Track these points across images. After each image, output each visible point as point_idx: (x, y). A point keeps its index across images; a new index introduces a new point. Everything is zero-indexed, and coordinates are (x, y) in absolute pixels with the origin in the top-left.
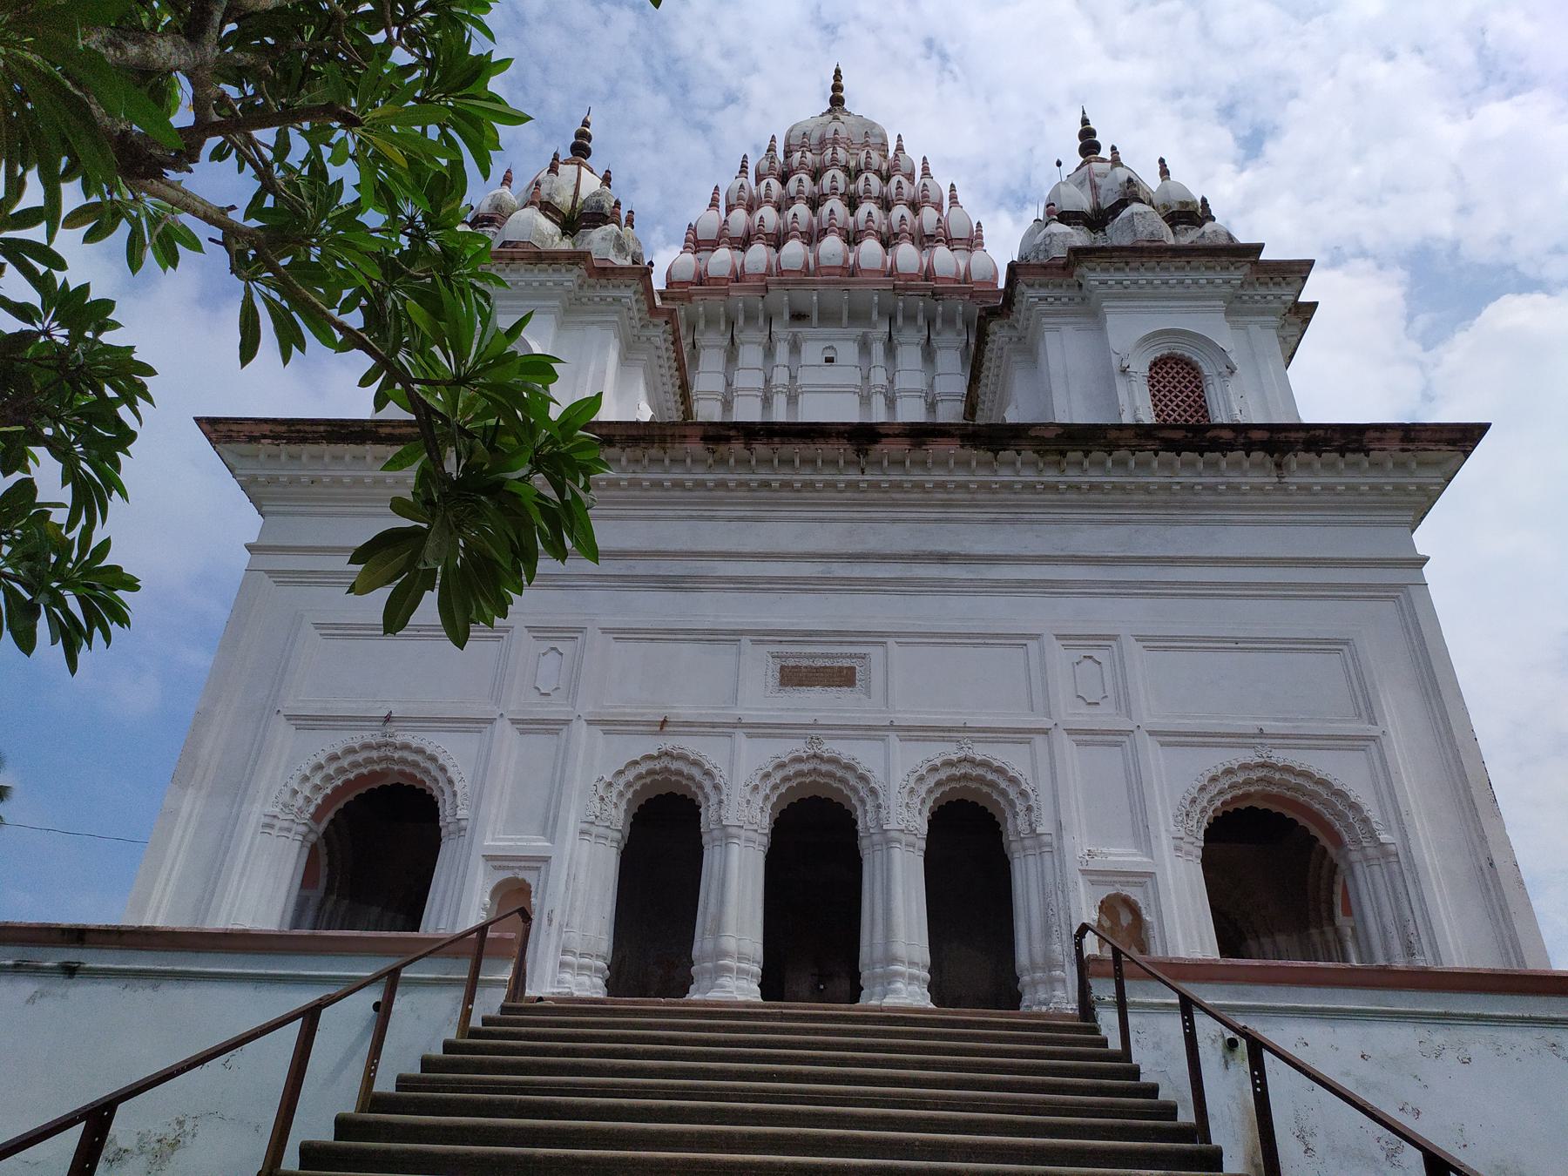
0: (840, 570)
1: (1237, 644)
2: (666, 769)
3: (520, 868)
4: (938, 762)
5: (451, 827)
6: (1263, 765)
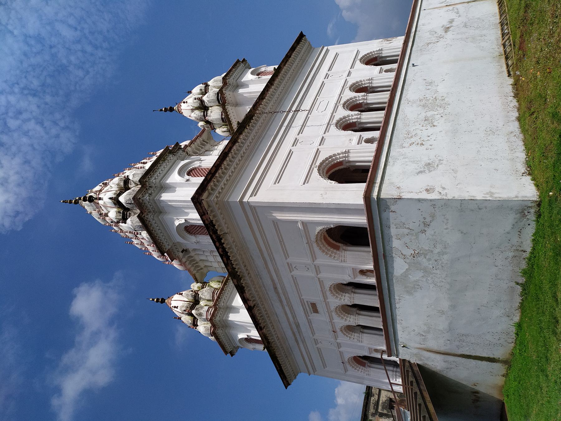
0: (285, 303)
1: (282, 241)
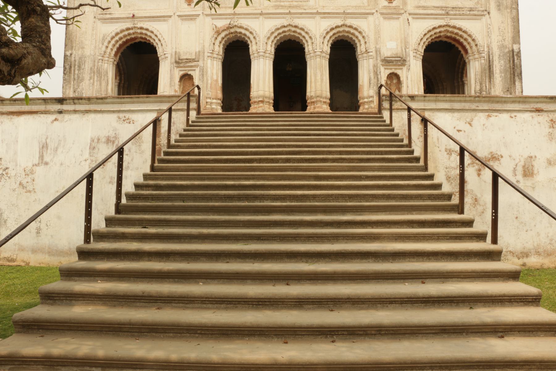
2: (236, 32)
3: (189, 70)
4: (334, 26)
5: (163, 57)
6: (447, 26)
